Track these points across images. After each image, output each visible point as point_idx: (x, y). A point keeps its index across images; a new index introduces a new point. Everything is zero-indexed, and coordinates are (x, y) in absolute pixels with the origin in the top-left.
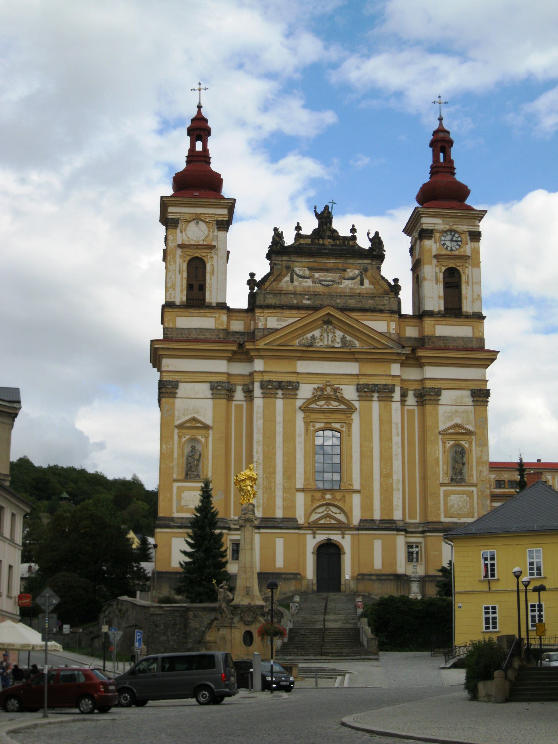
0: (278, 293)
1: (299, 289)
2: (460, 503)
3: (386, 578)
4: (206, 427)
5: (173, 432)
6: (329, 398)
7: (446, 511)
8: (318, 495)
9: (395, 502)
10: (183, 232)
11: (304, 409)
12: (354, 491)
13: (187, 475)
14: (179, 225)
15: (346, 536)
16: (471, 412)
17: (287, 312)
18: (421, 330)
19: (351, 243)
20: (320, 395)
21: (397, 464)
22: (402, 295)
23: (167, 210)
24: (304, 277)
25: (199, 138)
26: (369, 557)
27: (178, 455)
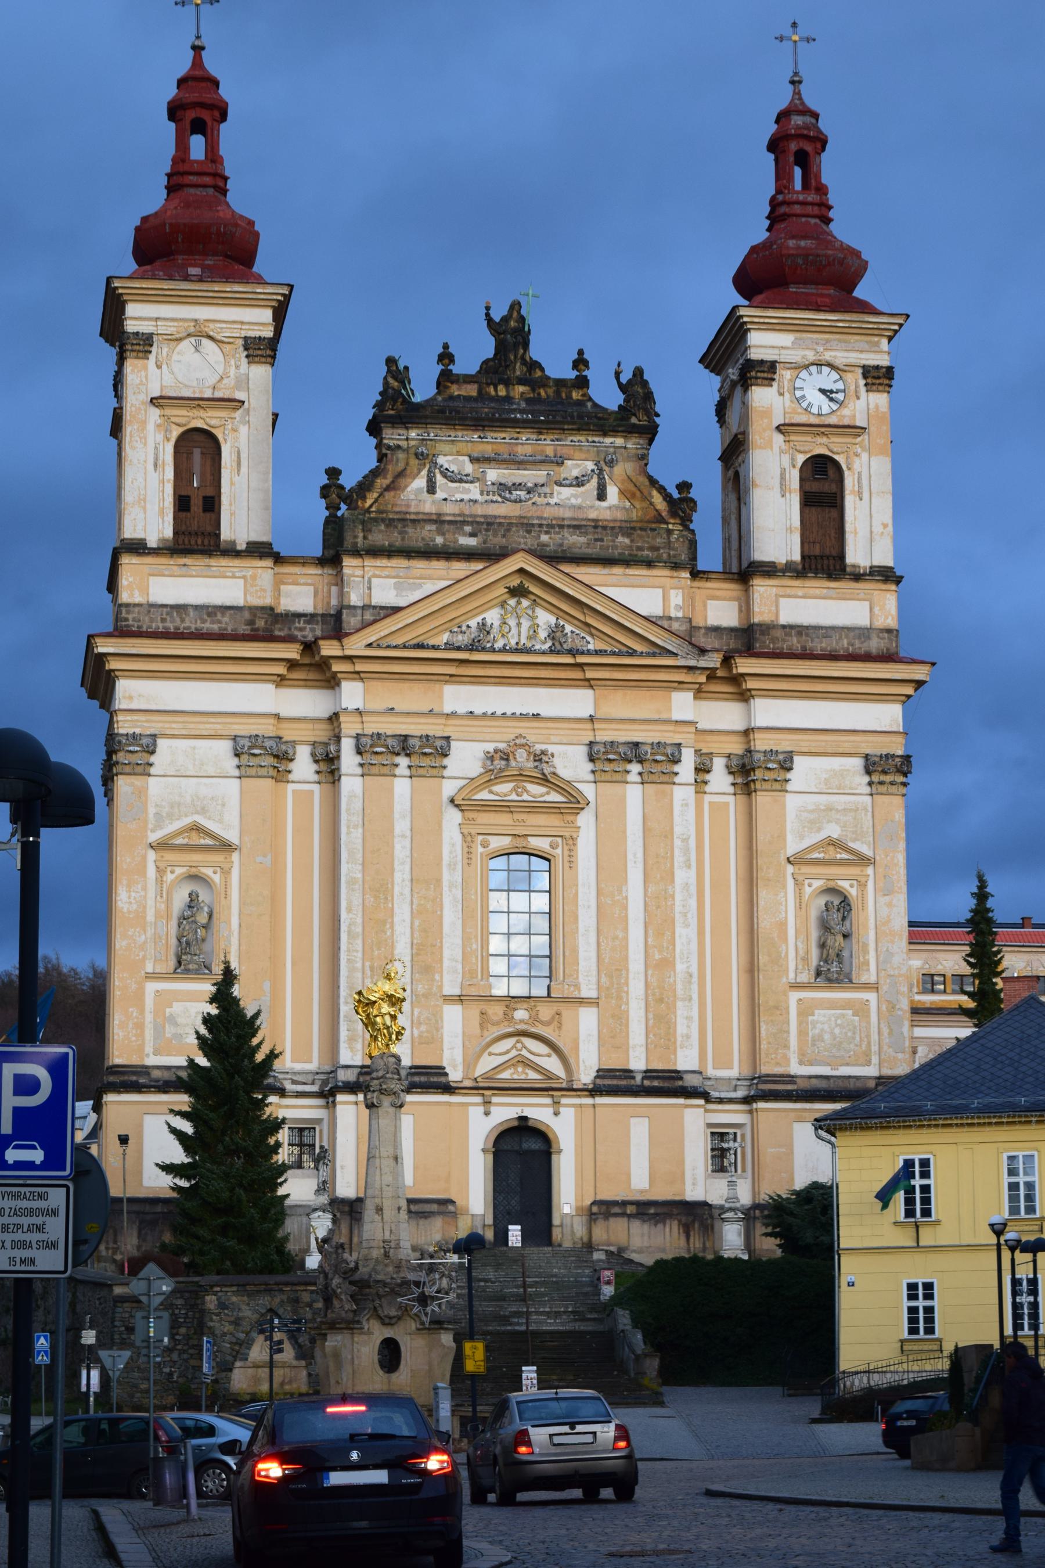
0: (399, 520)
1: (449, 509)
2: (837, 1031)
4: (226, 847)
5: (144, 858)
6: (521, 775)
9: (681, 1029)
10: (164, 366)
12: (583, 1001)
13: (179, 963)
14: (154, 349)
15: (562, 1110)
16: (865, 809)
17: (419, 565)
18: (746, 607)
19: (576, 395)
20: (501, 770)
21: (685, 935)
22: (698, 522)
23: (123, 312)
25: (199, 127)
26: (618, 1160)
27: (158, 915)
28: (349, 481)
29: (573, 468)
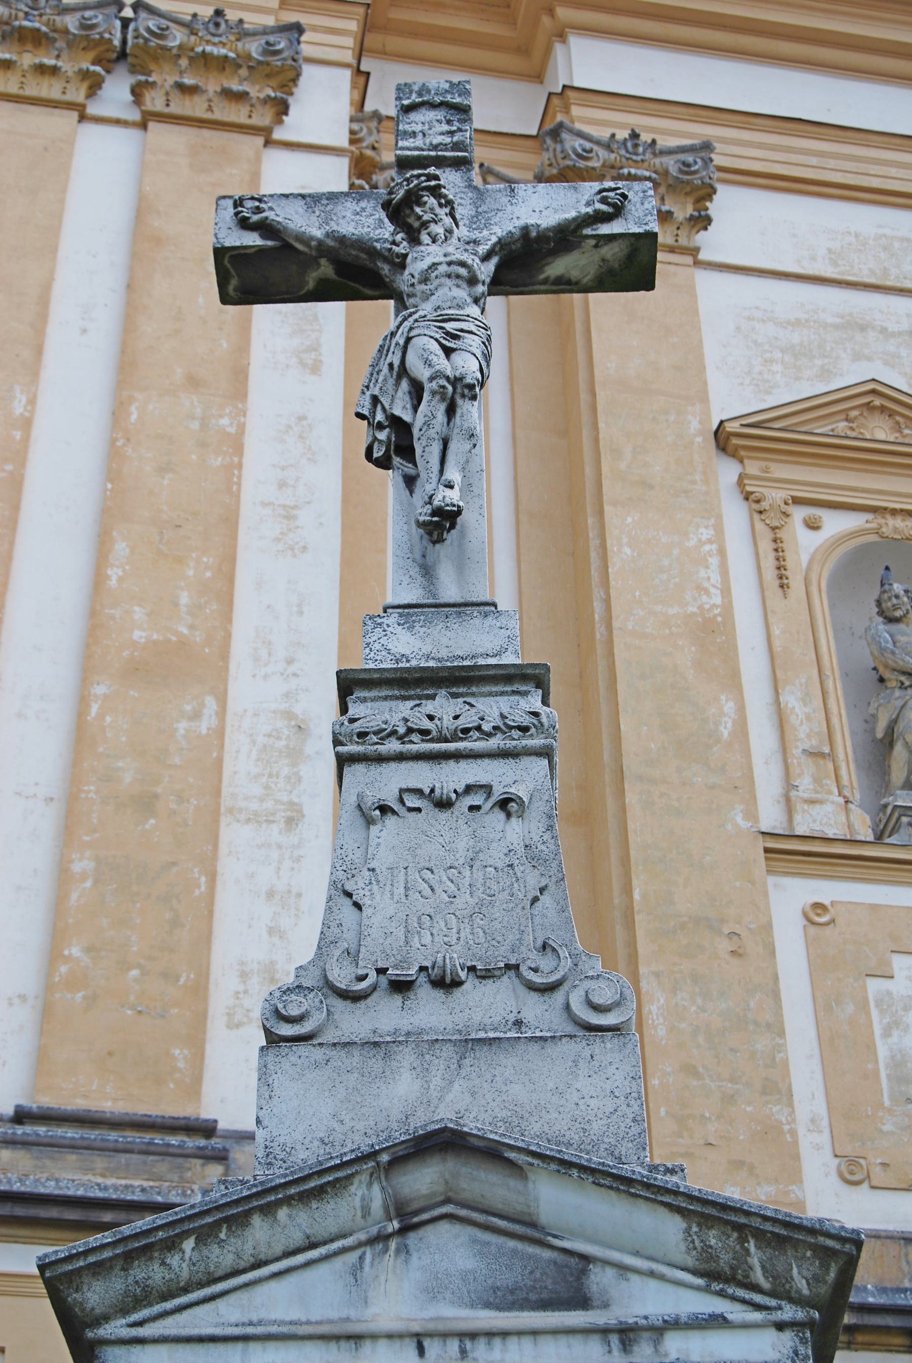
7: (848, 1111)
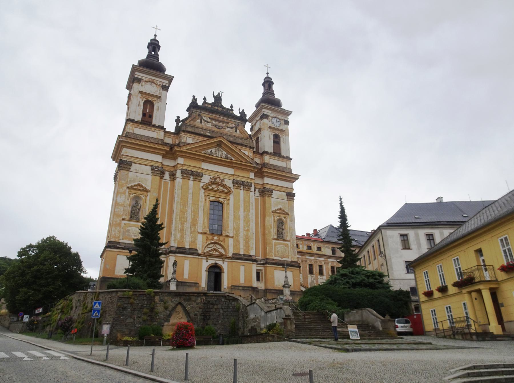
3: (247, 288)
4: (147, 191)
8: (210, 237)
11: (205, 188)
12: (230, 237)
13: (131, 217)
18: (262, 159)
24: (207, 122)
28: (181, 119)
29: (230, 125)
